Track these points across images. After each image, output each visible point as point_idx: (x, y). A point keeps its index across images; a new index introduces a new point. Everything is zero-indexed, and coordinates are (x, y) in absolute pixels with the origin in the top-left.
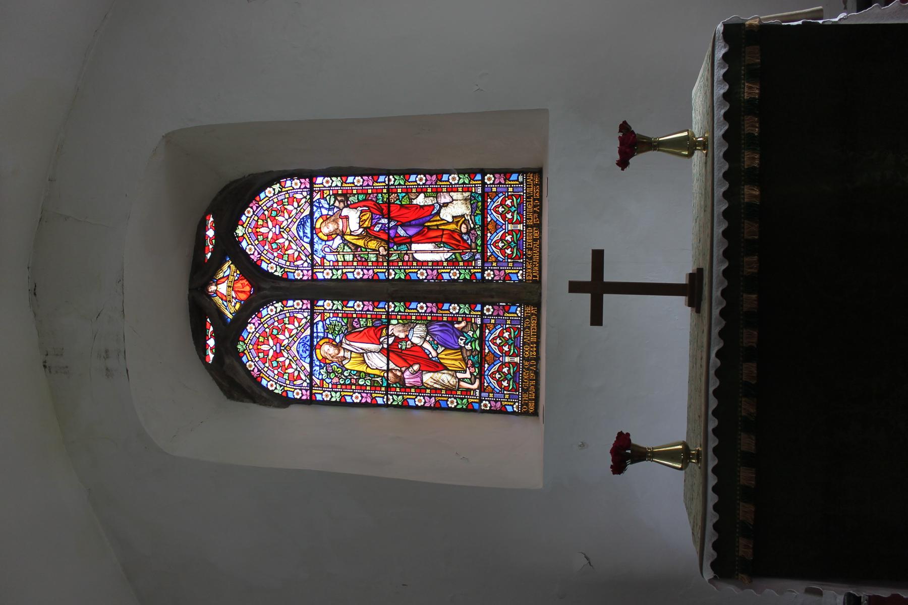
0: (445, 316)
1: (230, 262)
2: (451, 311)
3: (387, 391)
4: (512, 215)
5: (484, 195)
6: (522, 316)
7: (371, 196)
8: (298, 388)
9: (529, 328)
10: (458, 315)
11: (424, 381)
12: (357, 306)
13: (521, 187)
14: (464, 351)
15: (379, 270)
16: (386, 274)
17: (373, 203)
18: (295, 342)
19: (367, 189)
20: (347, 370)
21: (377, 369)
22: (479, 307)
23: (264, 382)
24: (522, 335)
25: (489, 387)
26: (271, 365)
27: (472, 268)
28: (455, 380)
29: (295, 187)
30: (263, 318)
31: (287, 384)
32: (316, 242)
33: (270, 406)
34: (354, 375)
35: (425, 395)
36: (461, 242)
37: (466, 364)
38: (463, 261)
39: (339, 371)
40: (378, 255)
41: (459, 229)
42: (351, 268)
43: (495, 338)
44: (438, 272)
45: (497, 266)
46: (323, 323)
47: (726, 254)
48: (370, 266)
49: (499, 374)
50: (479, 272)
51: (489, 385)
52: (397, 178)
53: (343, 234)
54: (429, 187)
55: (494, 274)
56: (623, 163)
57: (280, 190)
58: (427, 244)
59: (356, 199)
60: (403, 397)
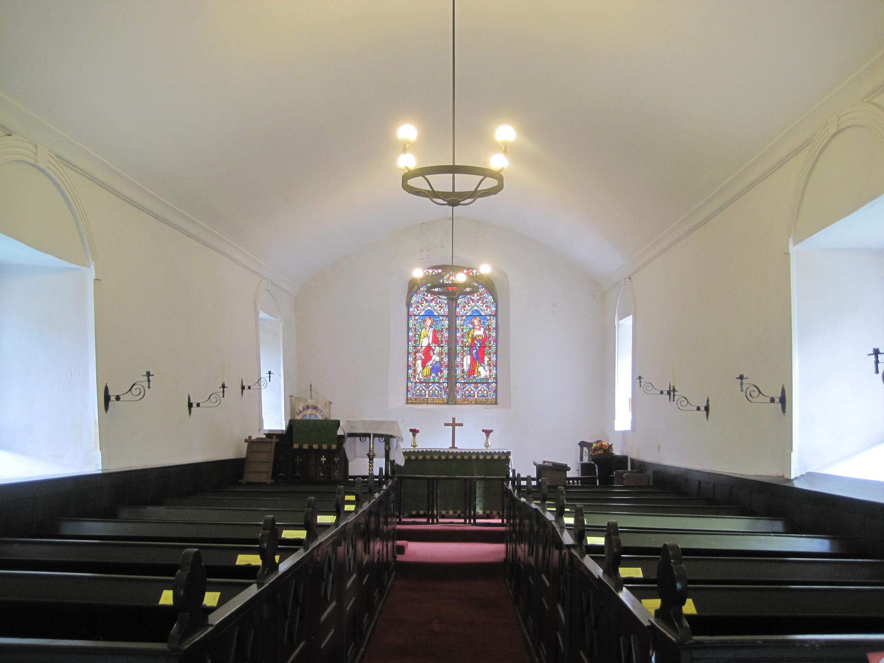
5: (488, 383)
12: (446, 335)
37: (425, 377)
47: (461, 452)
56: (483, 431)
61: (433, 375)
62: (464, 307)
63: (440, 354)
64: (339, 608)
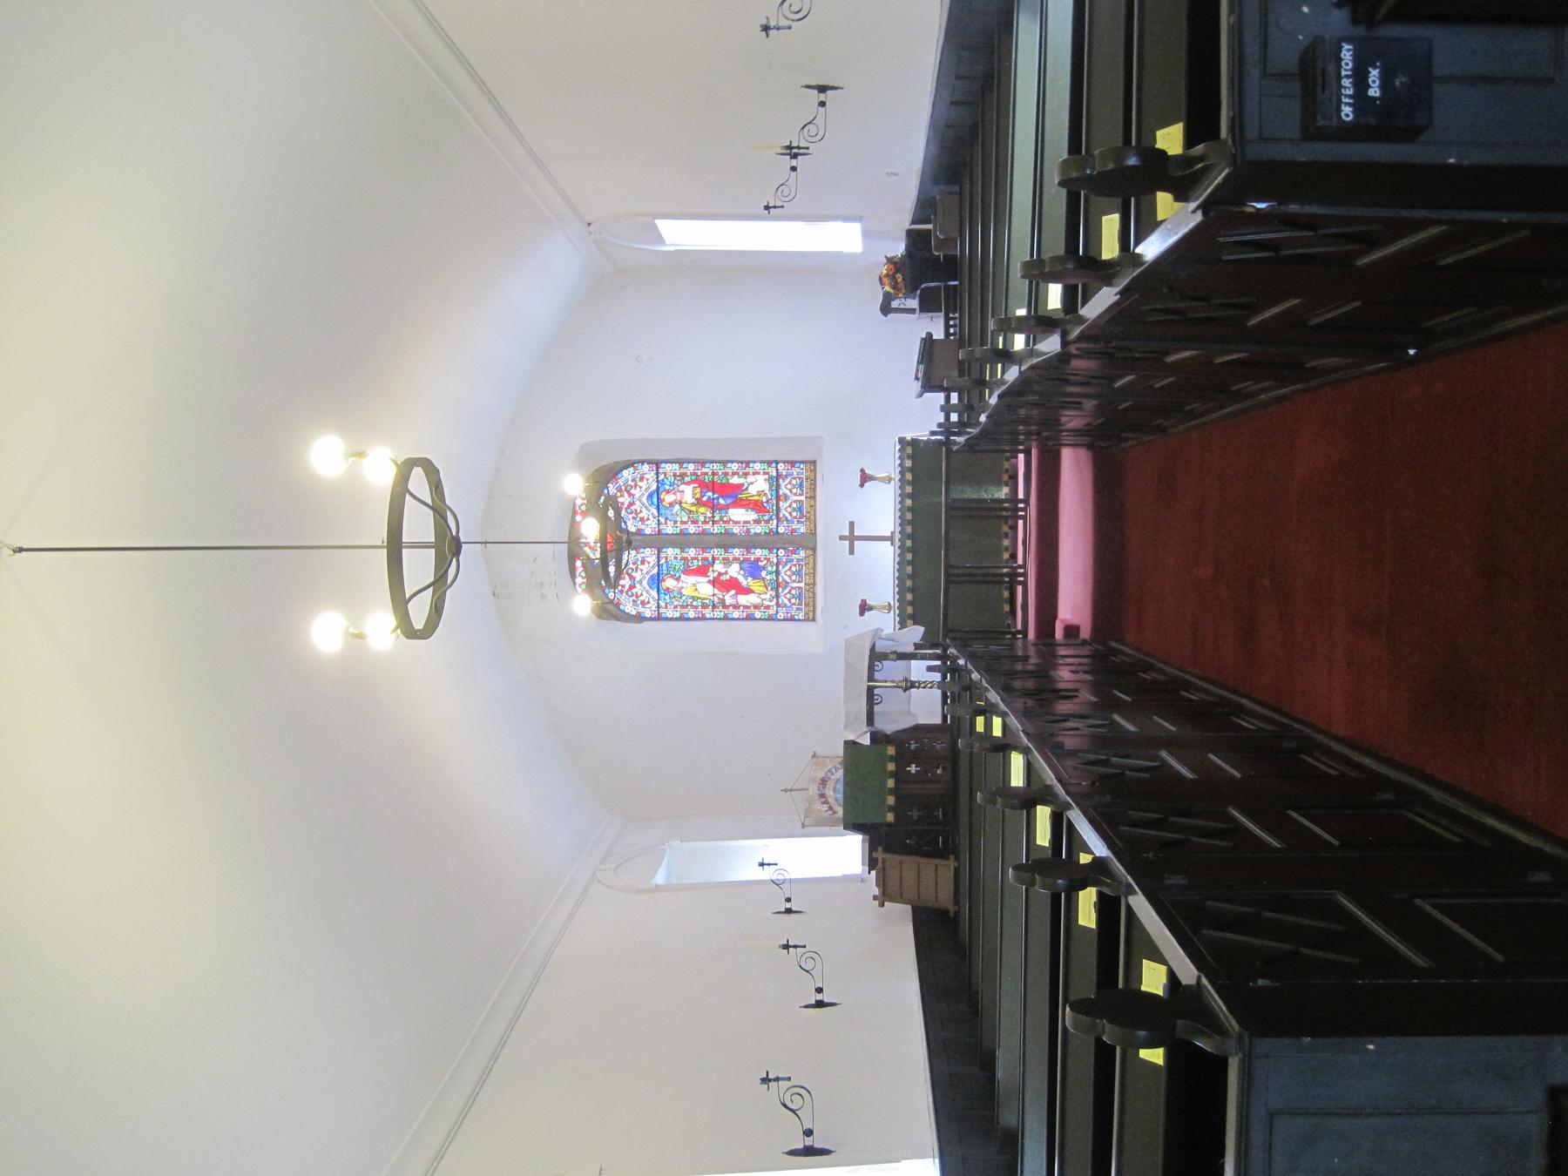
5: (778, 476)
12: (692, 552)
22: (775, 551)
37: (767, 589)
56: (862, 485)
61: (763, 574)
62: (642, 520)
63: (727, 562)
64: (1170, 744)
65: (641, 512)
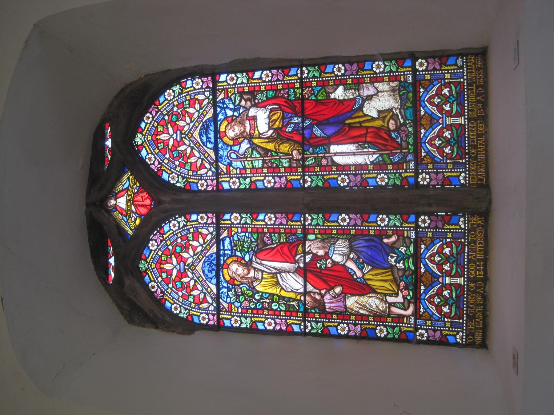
0: (372, 230)
1: (130, 173)
2: (379, 223)
3: (304, 317)
4: (450, 107)
5: (417, 83)
6: (466, 228)
7: (282, 91)
8: (204, 312)
9: (475, 242)
10: (387, 228)
11: (347, 306)
13: (460, 72)
14: (396, 271)
15: (293, 177)
16: (301, 181)
17: (284, 100)
18: (200, 260)
19: (277, 84)
20: (258, 292)
21: (292, 291)
23: (168, 304)
24: (466, 251)
25: (426, 313)
26: (175, 285)
27: (403, 171)
28: (384, 305)
29: (197, 88)
30: (166, 234)
31: (192, 308)
32: (220, 147)
33: (174, 332)
34: (267, 298)
35: (349, 322)
36: (390, 141)
37: (398, 286)
38: (392, 163)
39: (249, 293)
40: (292, 160)
41: (386, 125)
42: (261, 176)
43: (433, 255)
44: (362, 178)
45: (433, 169)
46: (230, 239)
48: (282, 173)
49: (439, 298)
50: (412, 176)
51: (426, 311)
52: (311, 70)
53: (250, 137)
54: (349, 78)
55: (430, 178)
57: (180, 92)
58: (348, 145)
59: (264, 96)
60: (323, 324)
65: (192, 155)
